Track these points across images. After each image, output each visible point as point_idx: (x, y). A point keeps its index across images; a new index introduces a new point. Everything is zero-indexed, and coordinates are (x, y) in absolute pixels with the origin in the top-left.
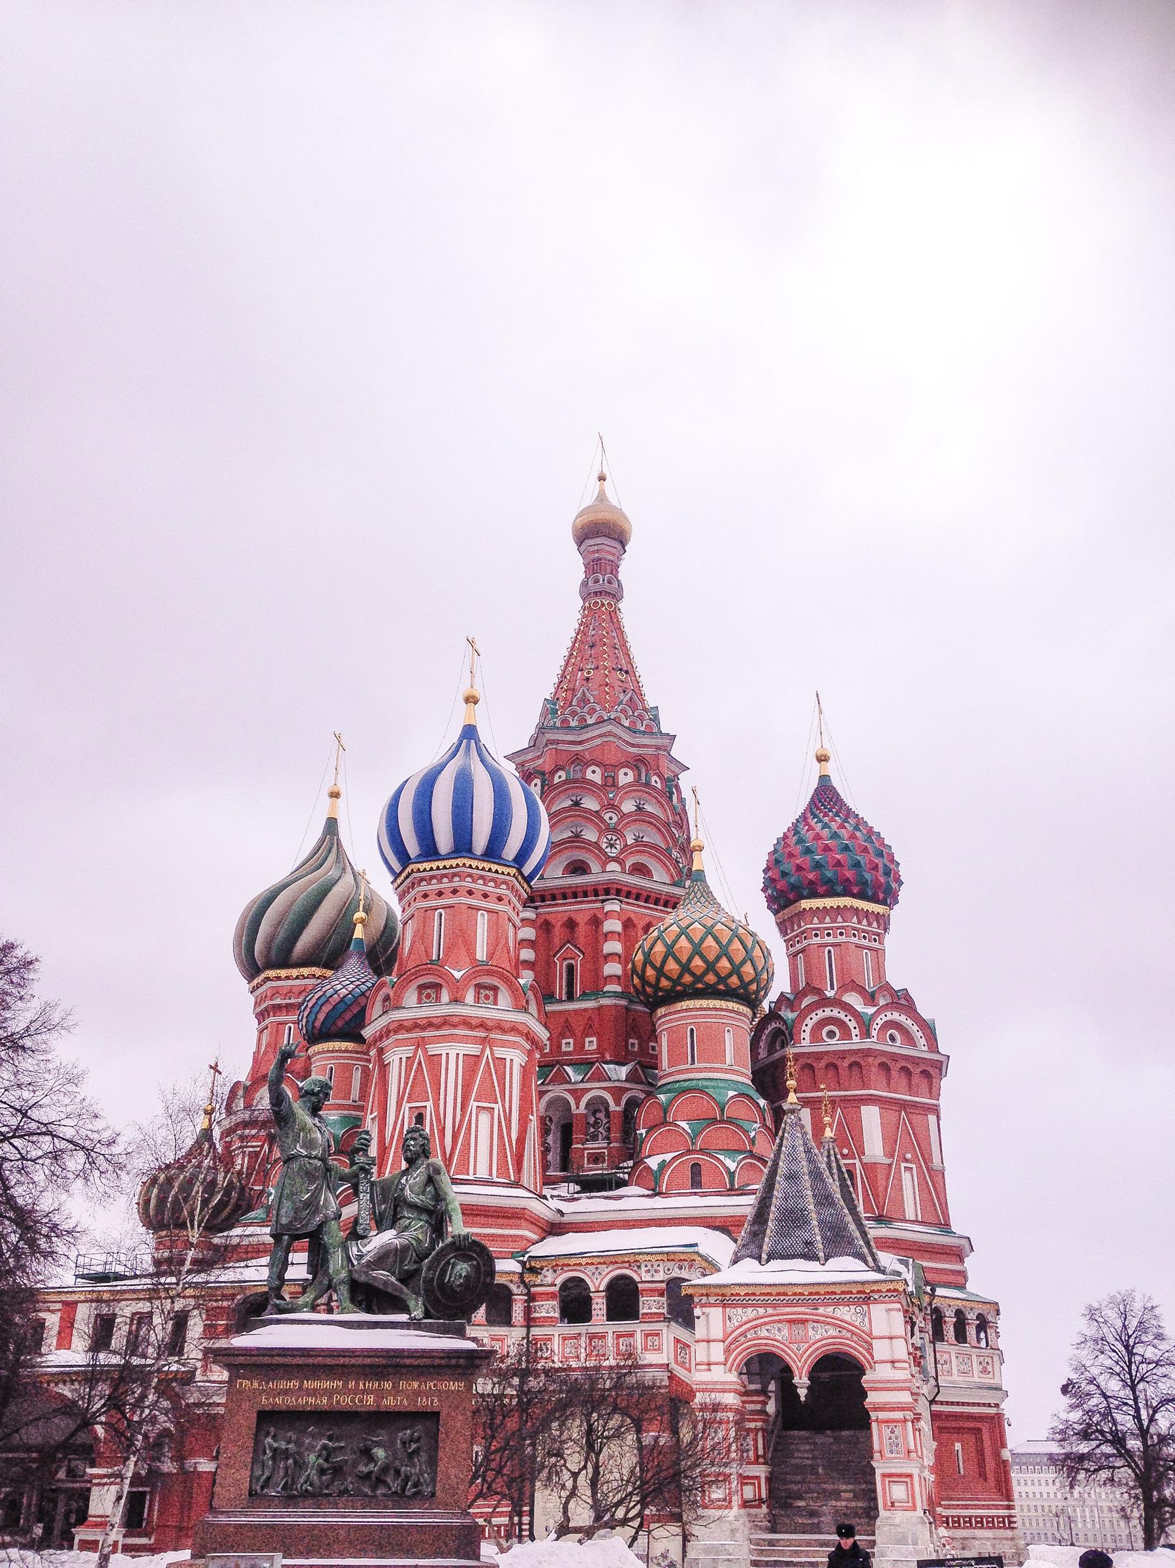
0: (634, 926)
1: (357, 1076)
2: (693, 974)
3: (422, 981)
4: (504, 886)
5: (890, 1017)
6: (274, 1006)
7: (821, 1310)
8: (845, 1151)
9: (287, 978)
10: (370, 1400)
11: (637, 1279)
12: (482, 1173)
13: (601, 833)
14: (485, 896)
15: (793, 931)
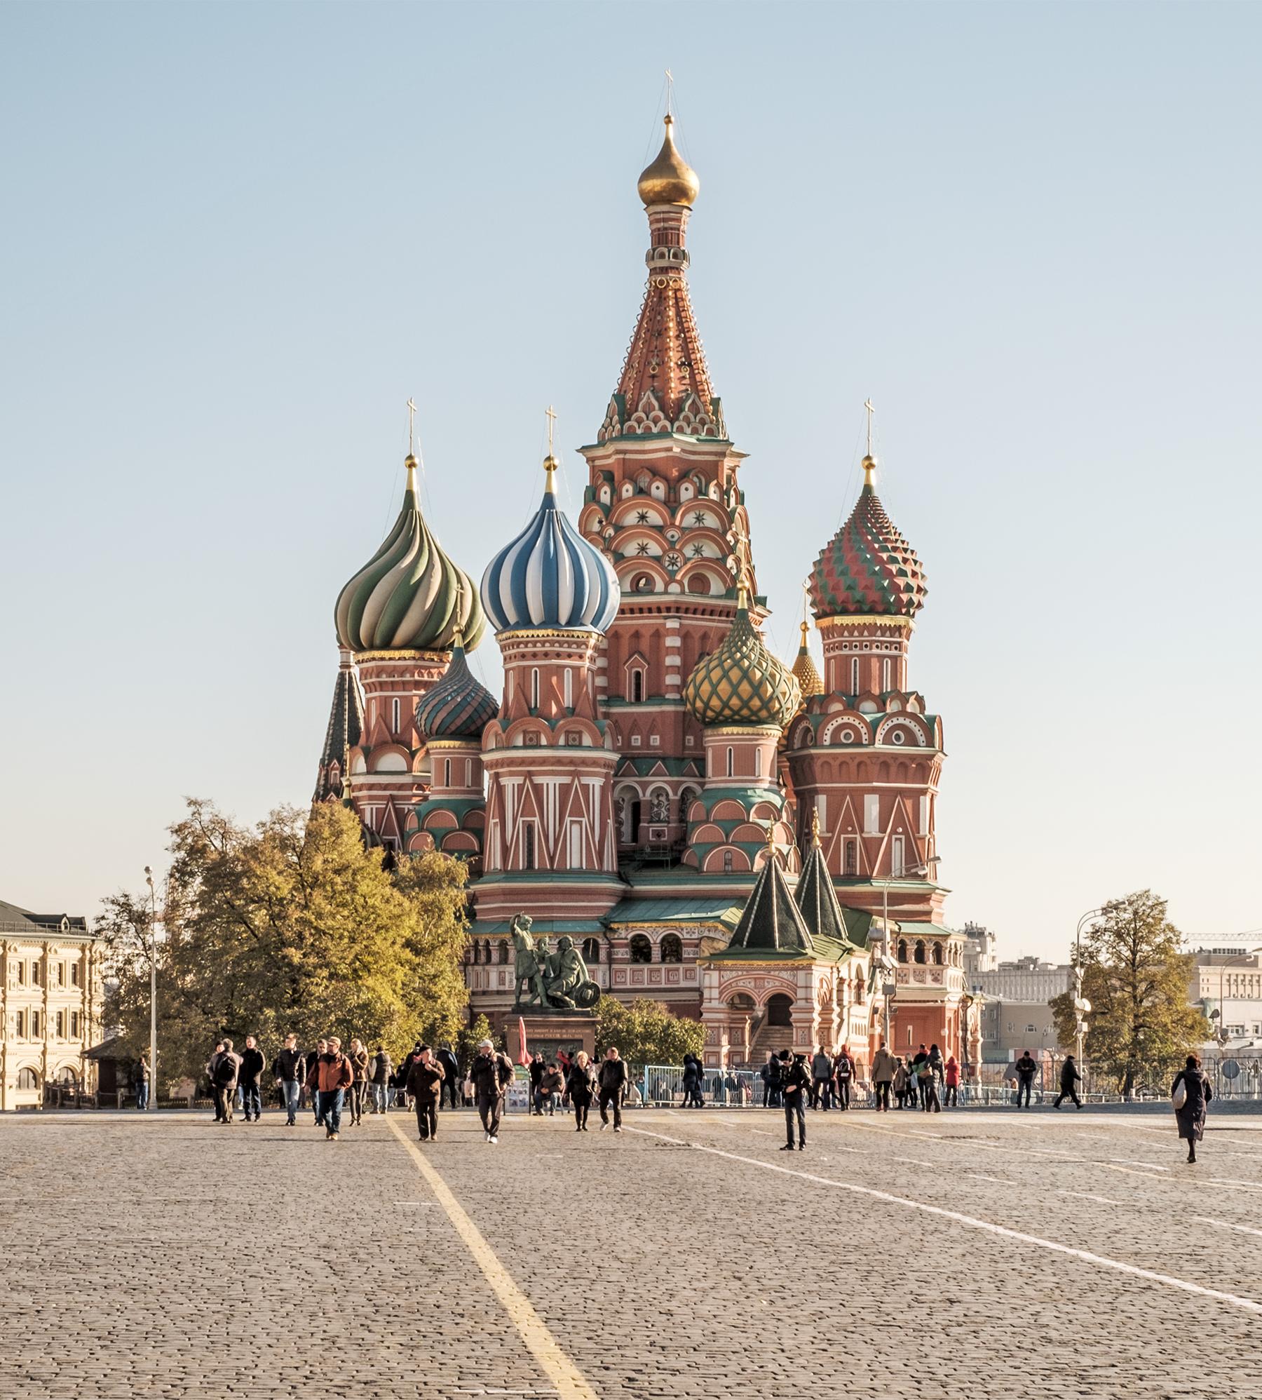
0: (693, 637)
1: (469, 767)
2: (731, 709)
3: (524, 727)
4: (584, 647)
5: (895, 721)
6: (381, 683)
7: (772, 973)
8: (850, 829)
9: (390, 659)
10: (558, 1036)
11: (681, 937)
12: (576, 864)
13: (665, 552)
14: (570, 656)
15: (829, 638)
